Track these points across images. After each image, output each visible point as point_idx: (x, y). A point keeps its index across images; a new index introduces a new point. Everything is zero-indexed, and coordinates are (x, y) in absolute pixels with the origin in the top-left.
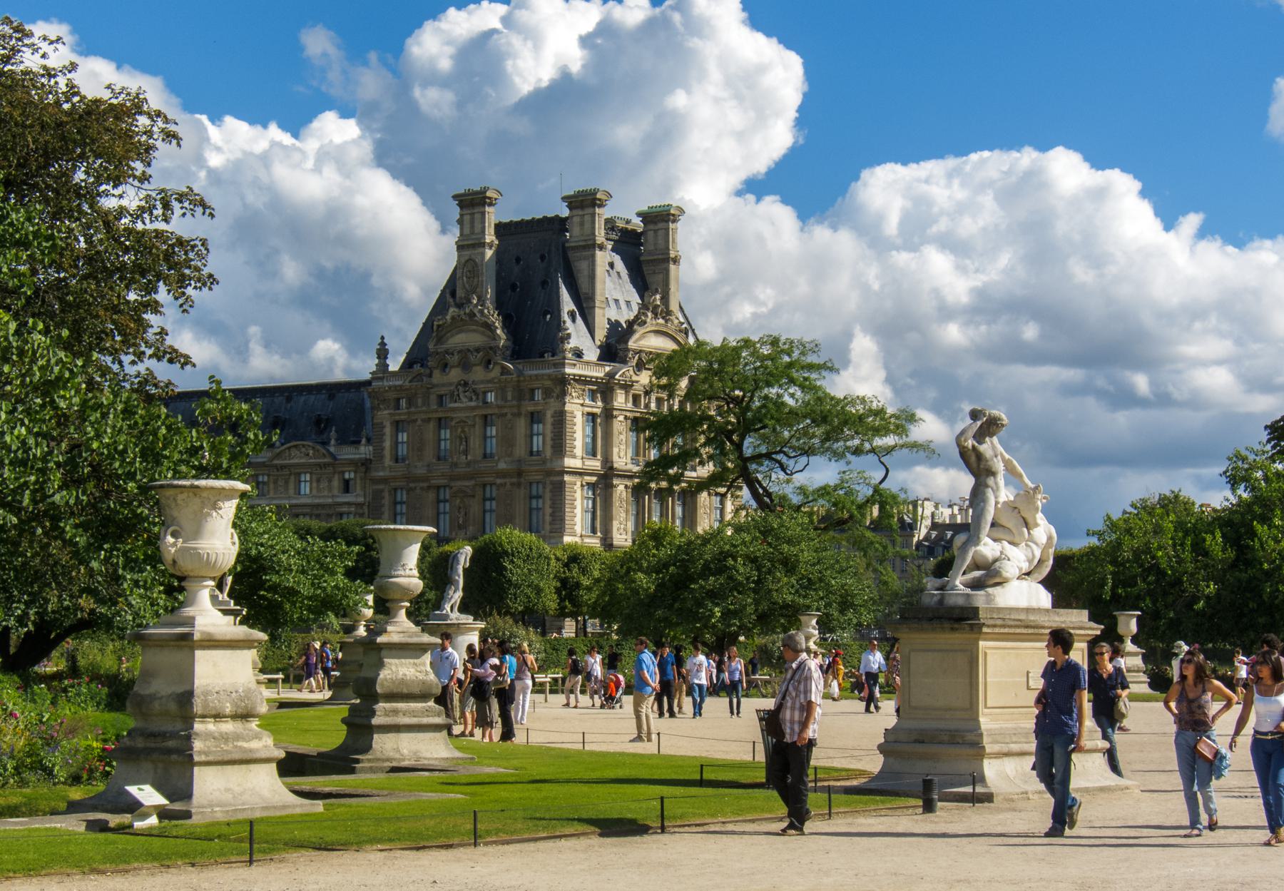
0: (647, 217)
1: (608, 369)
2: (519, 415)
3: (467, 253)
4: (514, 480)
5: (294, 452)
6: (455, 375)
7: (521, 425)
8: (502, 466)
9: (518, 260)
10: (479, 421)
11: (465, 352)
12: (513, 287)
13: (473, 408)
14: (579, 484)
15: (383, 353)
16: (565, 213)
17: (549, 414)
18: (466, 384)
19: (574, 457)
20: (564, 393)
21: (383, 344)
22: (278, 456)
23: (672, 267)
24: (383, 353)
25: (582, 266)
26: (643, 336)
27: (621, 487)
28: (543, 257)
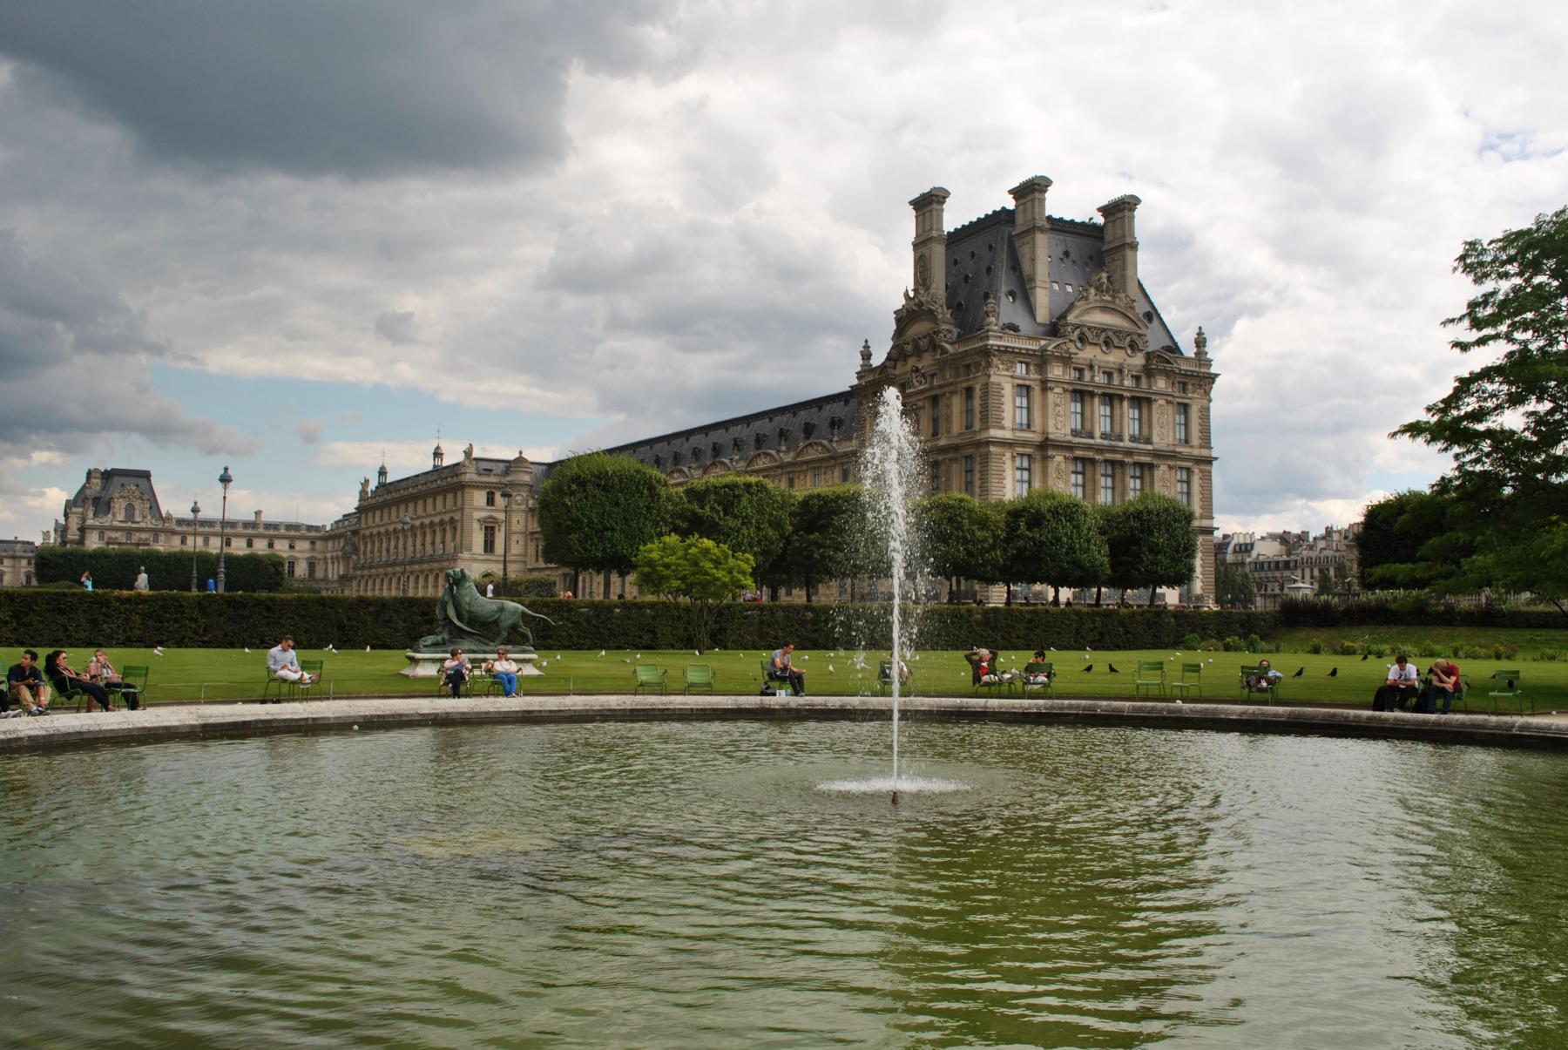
0: (1105, 210)
1: (1043, 343)
2: (955, 392)
3: (924, 250)
4: (951, 455)
5: (810, 450)
6: (911, 362)
7: (957, 404)
8: (942, 442)
9: (973, 254)
10: (928, 405)
11: (915, 342)
12: (967, 278)
13: (922, 392)
14: (1008, 455)
15: (866, 355)
16: (1010, 204)
17: (978, 387)
18: (917, 370)
19: (1003, 428)
20: (989, 365)
21: (867, 347)
22: (798, 455)
23: (1129, 253)
24: (866, 355)
25: (1024, 251)
26: (1087, 311)
27: (1059, 458)
28: (991, 247)
